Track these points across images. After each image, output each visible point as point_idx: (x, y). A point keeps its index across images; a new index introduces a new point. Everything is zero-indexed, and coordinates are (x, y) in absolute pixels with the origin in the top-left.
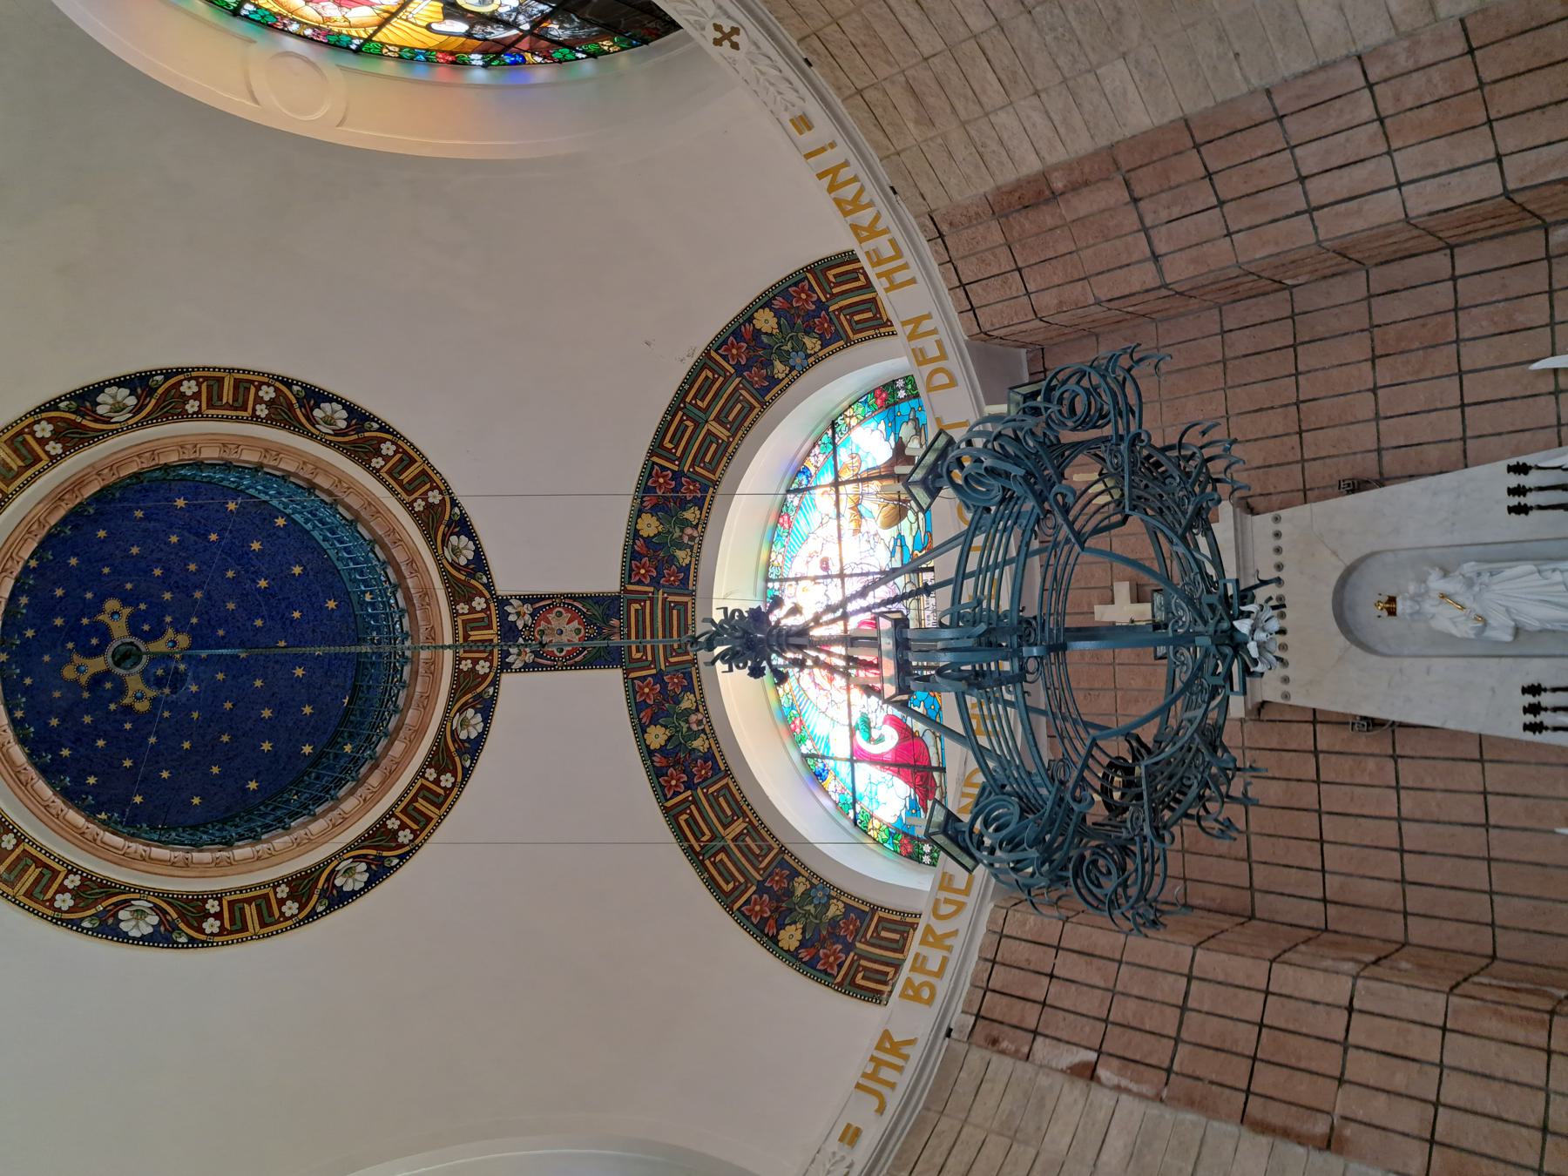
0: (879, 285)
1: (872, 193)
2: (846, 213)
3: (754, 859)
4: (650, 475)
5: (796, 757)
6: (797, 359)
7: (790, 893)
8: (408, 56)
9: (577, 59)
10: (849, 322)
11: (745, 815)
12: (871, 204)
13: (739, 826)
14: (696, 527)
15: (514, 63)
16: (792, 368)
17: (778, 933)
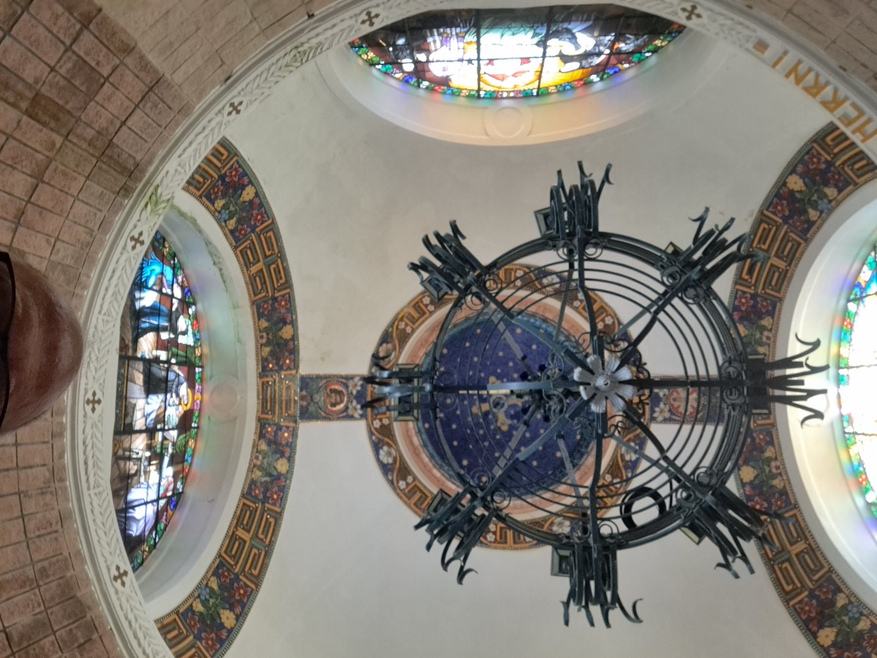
0: (856, 138)
1: (825, 76)
2: (814, 95)
3: (810, 572)
4: (736, 298)
5: (860, 502)
6: (823, 204)
7: (832, 603)
8: (563, 89)
9: (647, 57)
10: (852, 170)
11: (806, 539)
12: (827, 83)
13: (801, 546)
14: (770, 330)
15: (615, 72)
16: (821, 212)
17: (818, 631)
